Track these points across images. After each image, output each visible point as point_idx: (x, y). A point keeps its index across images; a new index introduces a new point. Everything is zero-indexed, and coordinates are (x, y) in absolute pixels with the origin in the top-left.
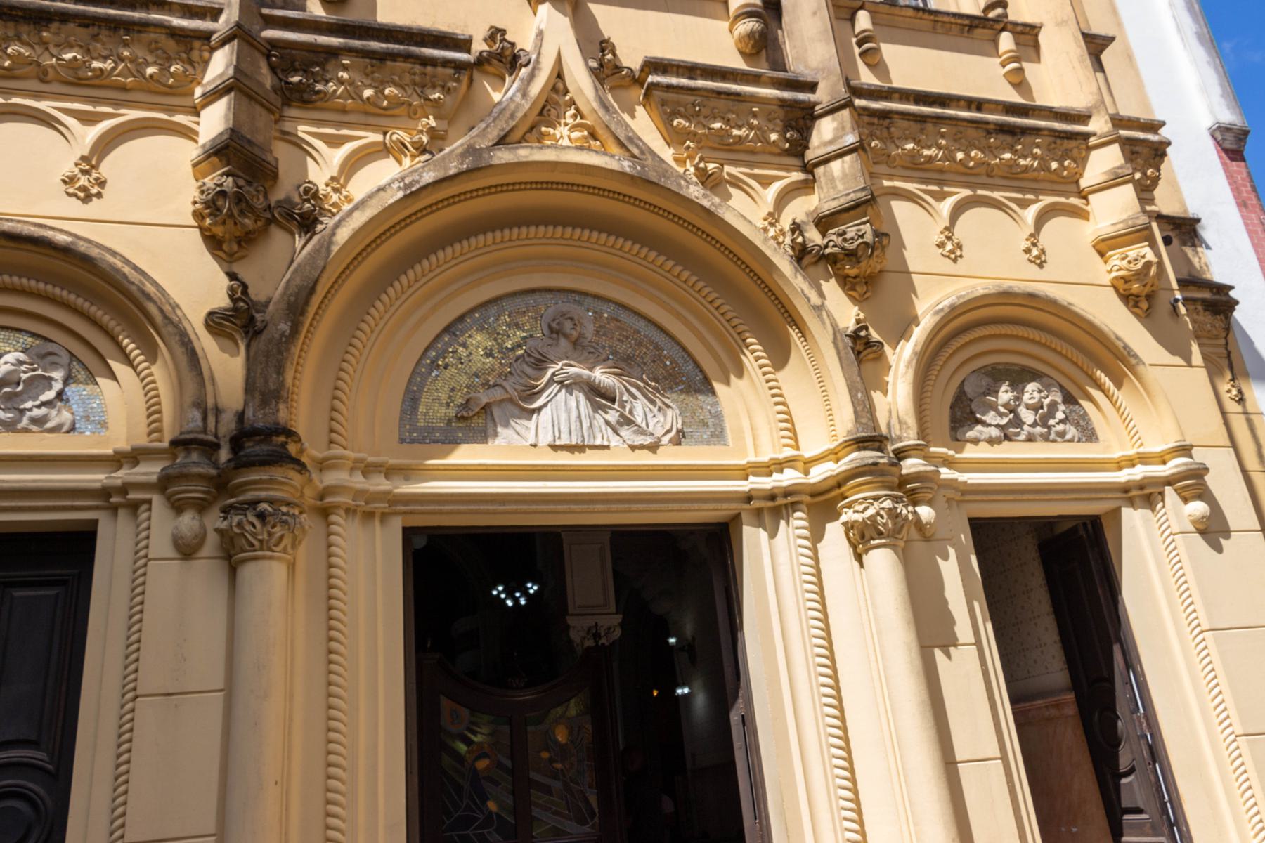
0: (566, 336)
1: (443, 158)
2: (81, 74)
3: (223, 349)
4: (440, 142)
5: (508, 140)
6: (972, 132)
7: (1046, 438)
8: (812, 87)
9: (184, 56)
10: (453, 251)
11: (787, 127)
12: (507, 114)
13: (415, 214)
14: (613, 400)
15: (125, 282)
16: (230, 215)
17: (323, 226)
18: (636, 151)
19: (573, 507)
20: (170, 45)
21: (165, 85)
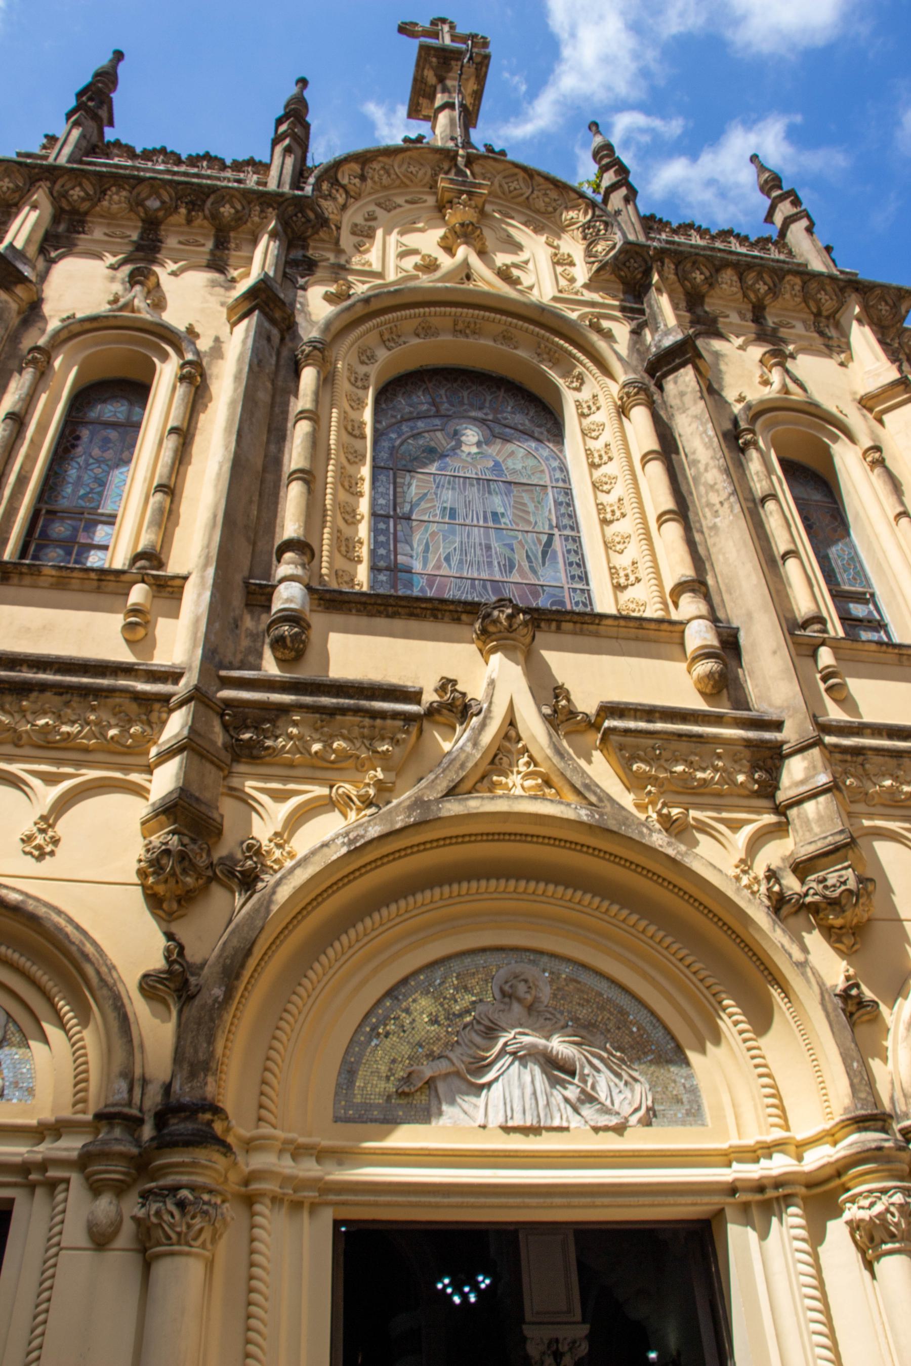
0: (520, 1000)
1: (390, 812)
2: (50, 738)
3: (154, 1014)
4: (387, 795)
5: (458, 790)
8: (778, 726)
9: (144, 717)
10: (398, 909)
11: (755, 767)
12: (457, 764)
13: (359, 869)
14: (572, 1074)
15: (66, 942)
16: (173, 874)
17: (264, 884)
18: (593, 799)
19: (527, 1200)
20: (133, 708)
21: (123, 746)
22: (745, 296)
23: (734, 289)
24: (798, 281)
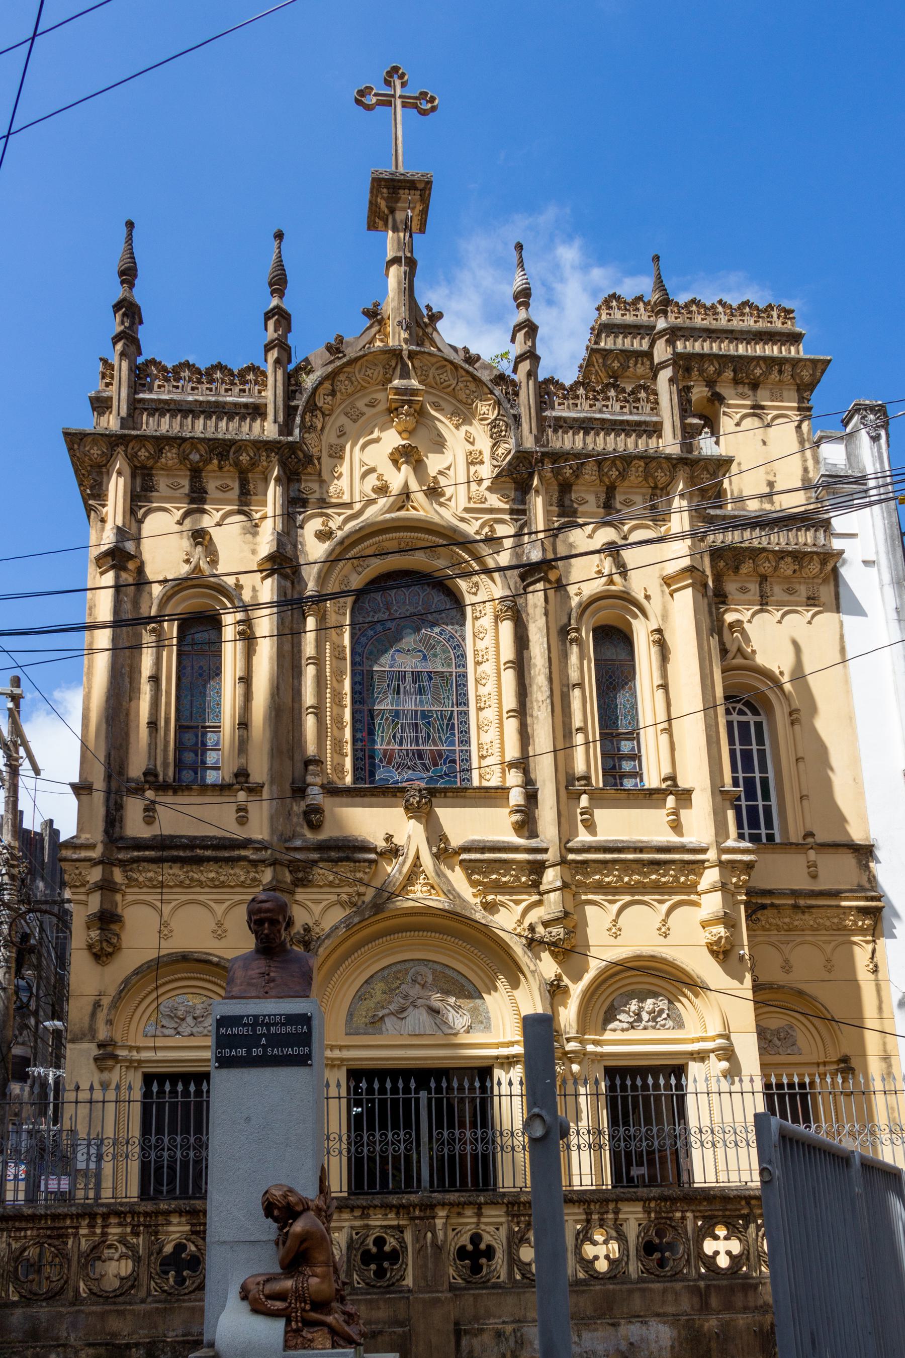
6: (634, 866)
7: (654, 1028)
8: (545, 851)
18: (451, 897)
22: (601, 481)
23: (594, 478)
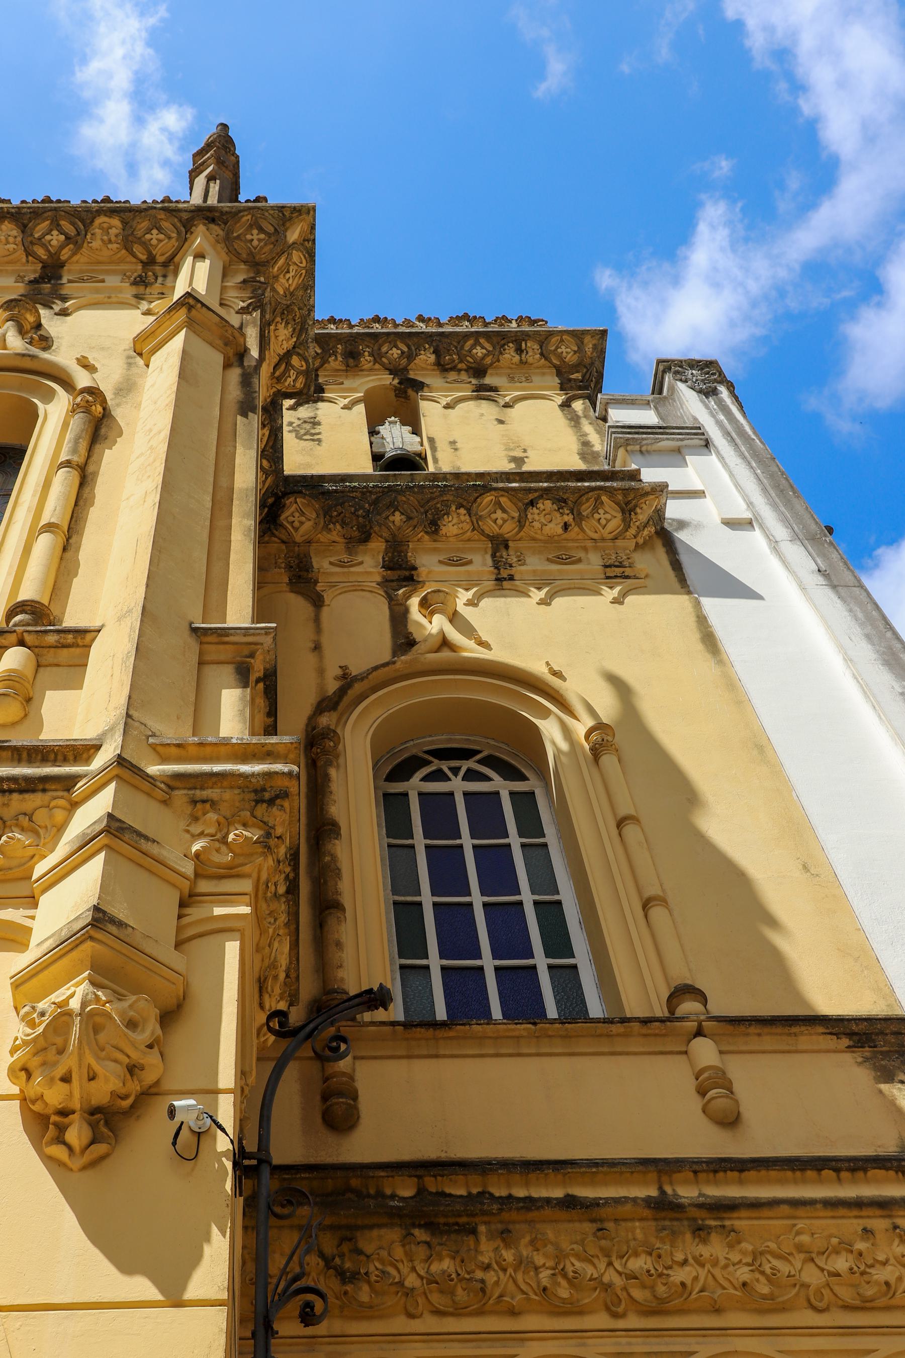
24: (116, 222)
